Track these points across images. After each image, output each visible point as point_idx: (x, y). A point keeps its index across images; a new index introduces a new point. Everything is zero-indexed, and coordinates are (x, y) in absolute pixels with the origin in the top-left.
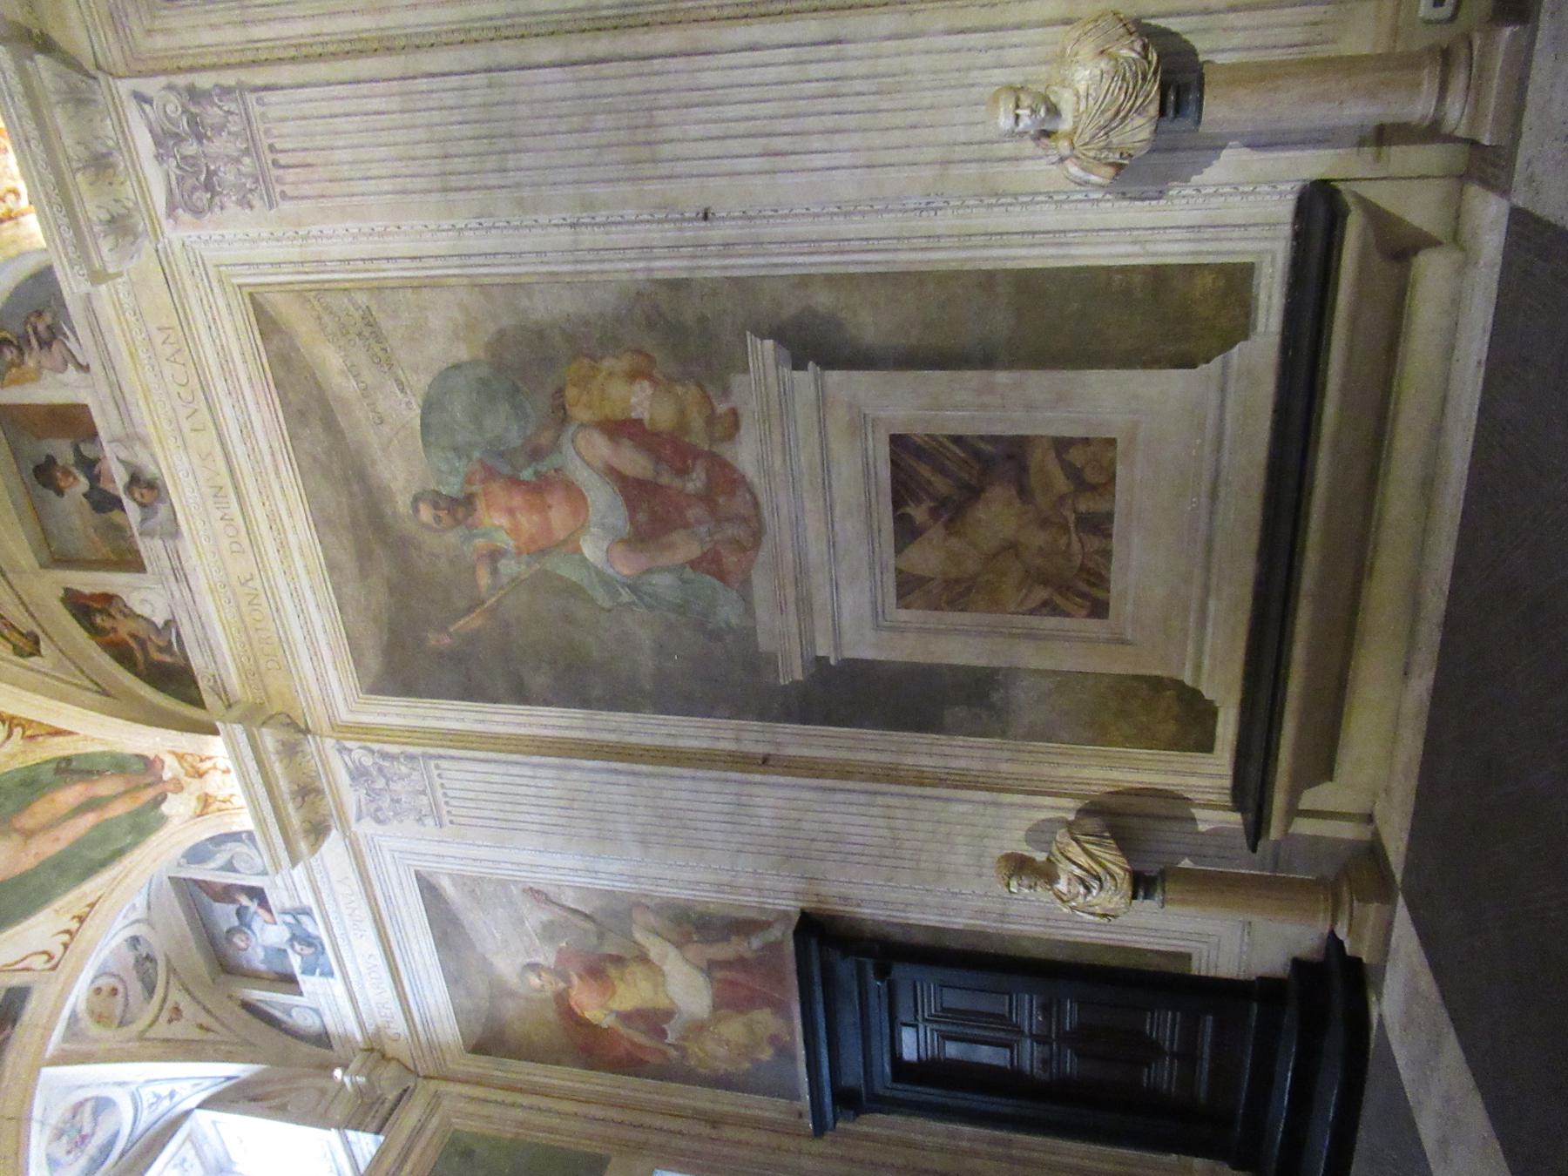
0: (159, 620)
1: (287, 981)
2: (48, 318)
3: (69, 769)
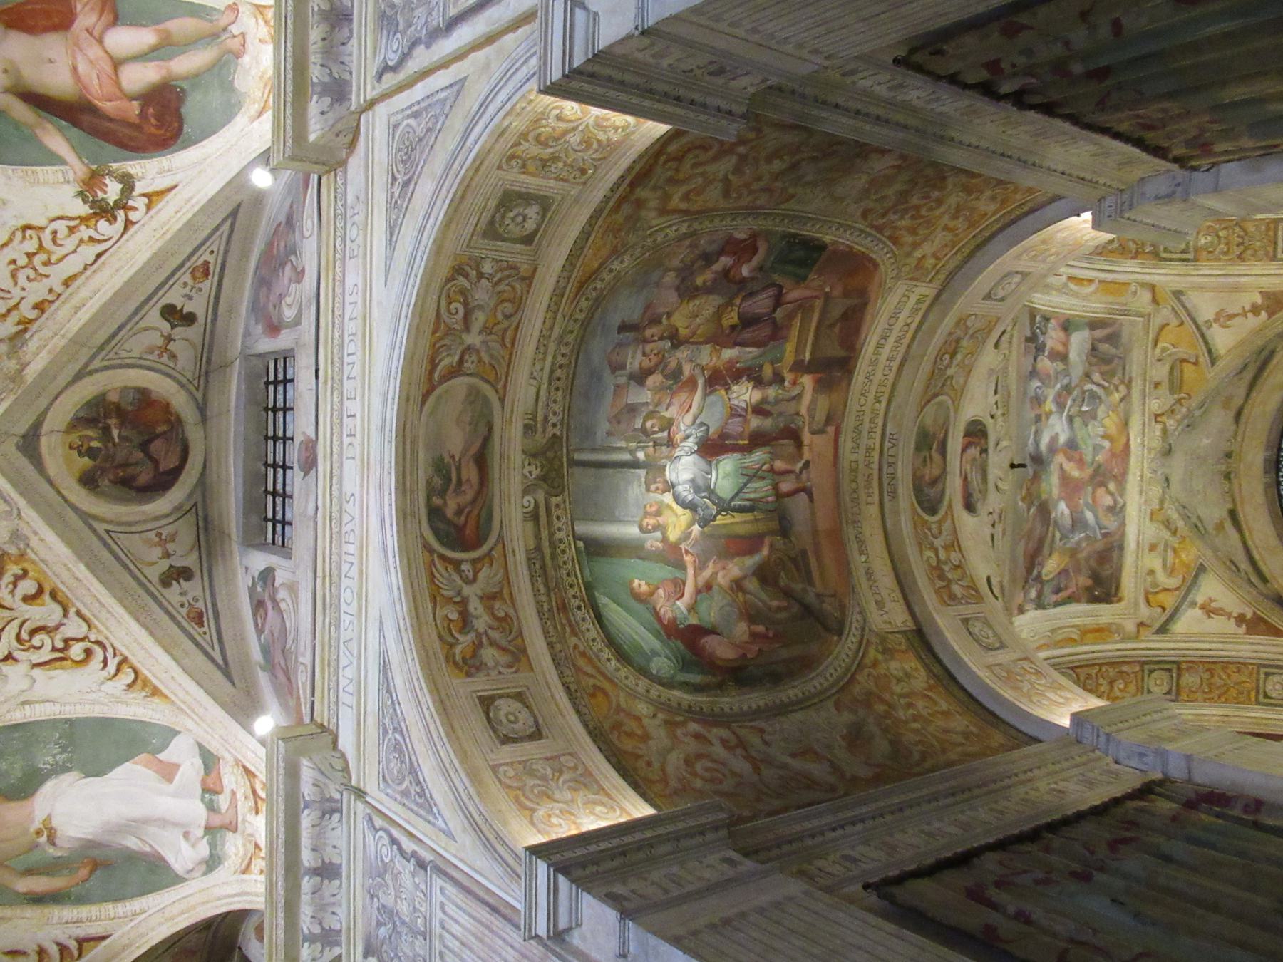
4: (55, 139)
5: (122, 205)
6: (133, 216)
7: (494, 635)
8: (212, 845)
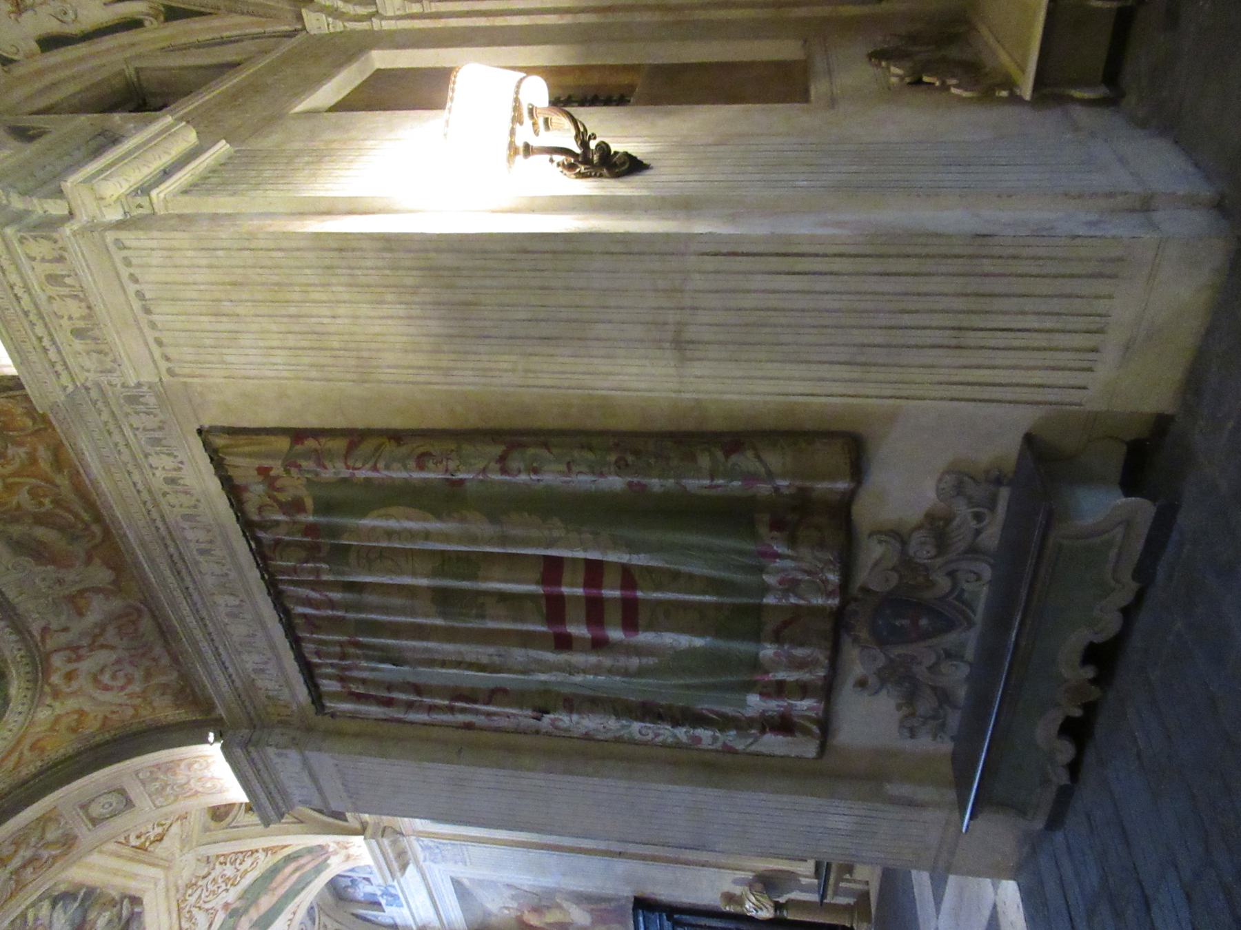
1: (376, 905)
3: (289, 859)
7: (33, 840)
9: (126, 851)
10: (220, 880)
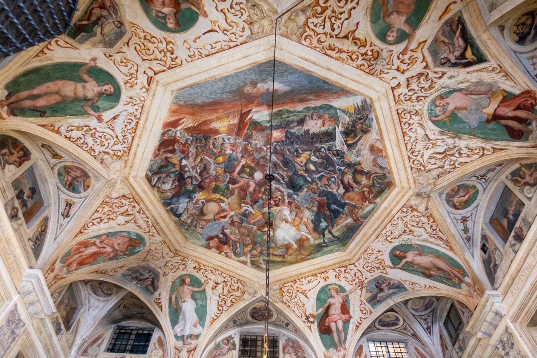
0: (7, 166)
2: (37, 246)
3: (41, 112)
4: (321, 310)
5: (309, 321)
6: (306, 323)
8: (180, 337)
9: (142, 206)
10: (98, 141)
